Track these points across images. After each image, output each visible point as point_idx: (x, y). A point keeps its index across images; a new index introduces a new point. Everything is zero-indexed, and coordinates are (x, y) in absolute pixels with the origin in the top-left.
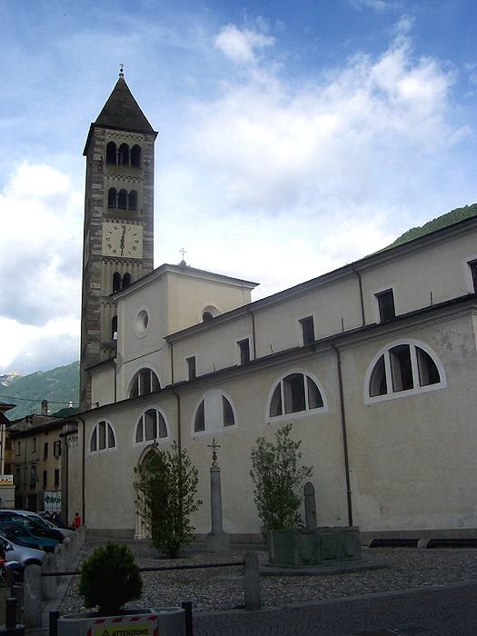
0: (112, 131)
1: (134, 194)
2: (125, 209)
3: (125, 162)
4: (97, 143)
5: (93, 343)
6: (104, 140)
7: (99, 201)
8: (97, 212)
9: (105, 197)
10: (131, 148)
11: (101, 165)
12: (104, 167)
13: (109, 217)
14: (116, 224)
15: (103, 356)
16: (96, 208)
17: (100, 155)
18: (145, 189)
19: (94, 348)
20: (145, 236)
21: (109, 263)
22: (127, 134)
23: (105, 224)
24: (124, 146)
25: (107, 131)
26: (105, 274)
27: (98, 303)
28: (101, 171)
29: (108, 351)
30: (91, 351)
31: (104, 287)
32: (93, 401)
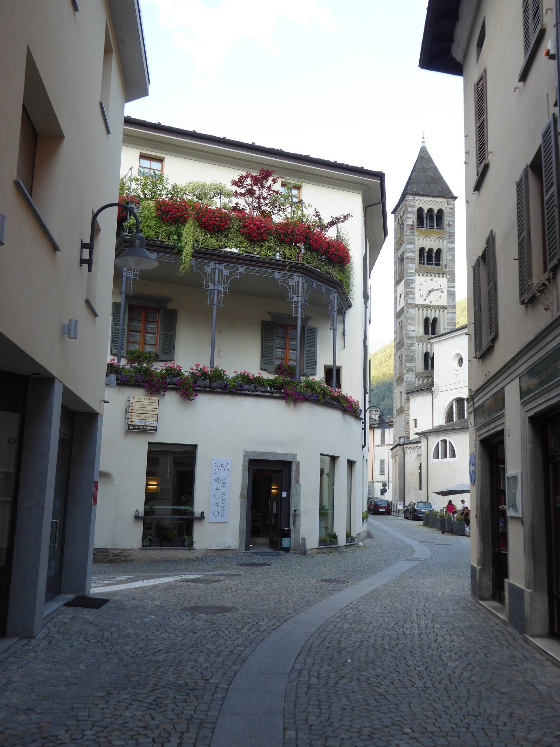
0: (421, 198)
1: (439, 251)
2: (431, 264)
3: (432, 227)
5: (410, 373)
6: (414, 206)
7: (411, 259)
8: (411, 268)
9: (416, 255)
10: (436, 212)
12: (415, 232)
13: (419, 272)
14: (425, 278)
15: (418, 383)
16: (410, 265)
17: (411, 219)
18: (448, 248)
19: (410, 377)
20: (448, 287)
21: (421, 309)
24: (430, 211)
25: (417, 198)
26: (419, 318)
27: (413, 342)
28: (413, 234)
29: (421, 379)
30: (409, 379)
31: (418, 329)
32: (412, 418)
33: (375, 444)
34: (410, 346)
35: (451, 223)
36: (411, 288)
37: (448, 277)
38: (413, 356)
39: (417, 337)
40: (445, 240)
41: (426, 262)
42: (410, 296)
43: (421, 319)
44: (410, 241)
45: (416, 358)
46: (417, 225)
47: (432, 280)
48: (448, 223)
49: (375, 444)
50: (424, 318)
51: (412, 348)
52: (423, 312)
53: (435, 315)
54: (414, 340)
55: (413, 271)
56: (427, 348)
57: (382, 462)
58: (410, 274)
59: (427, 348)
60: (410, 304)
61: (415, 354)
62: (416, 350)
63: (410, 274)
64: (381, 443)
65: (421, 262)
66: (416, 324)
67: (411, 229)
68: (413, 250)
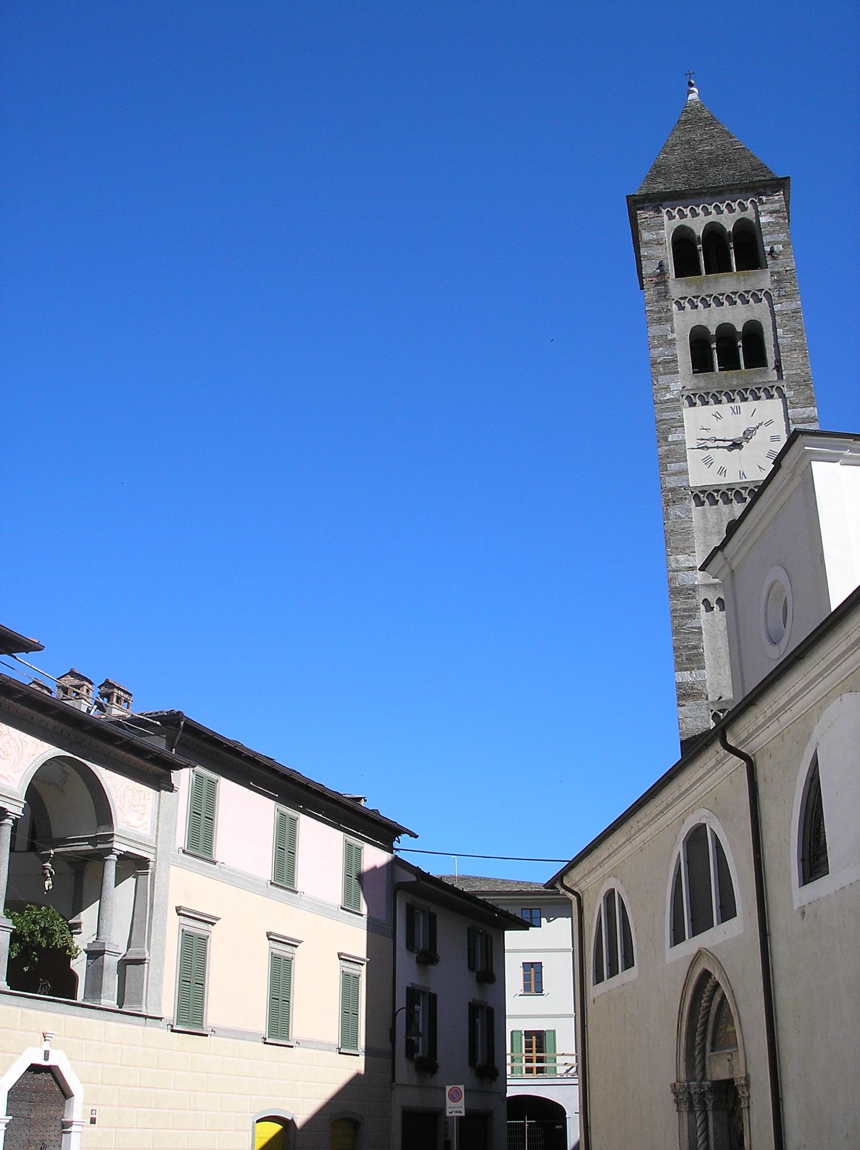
1: (753, 332)
5: (690, 703)
11: (664, 282)
14: (713, 408)
24: (713, 232)
34: (683, 617)
38: (695, 647)
41: (717, 367)
42: (673, 467)
46: (678, 275)
47: (738, 411)
60: (672, 490)
61: (701, 640)
65: (701, 363)
67: (657, 284)
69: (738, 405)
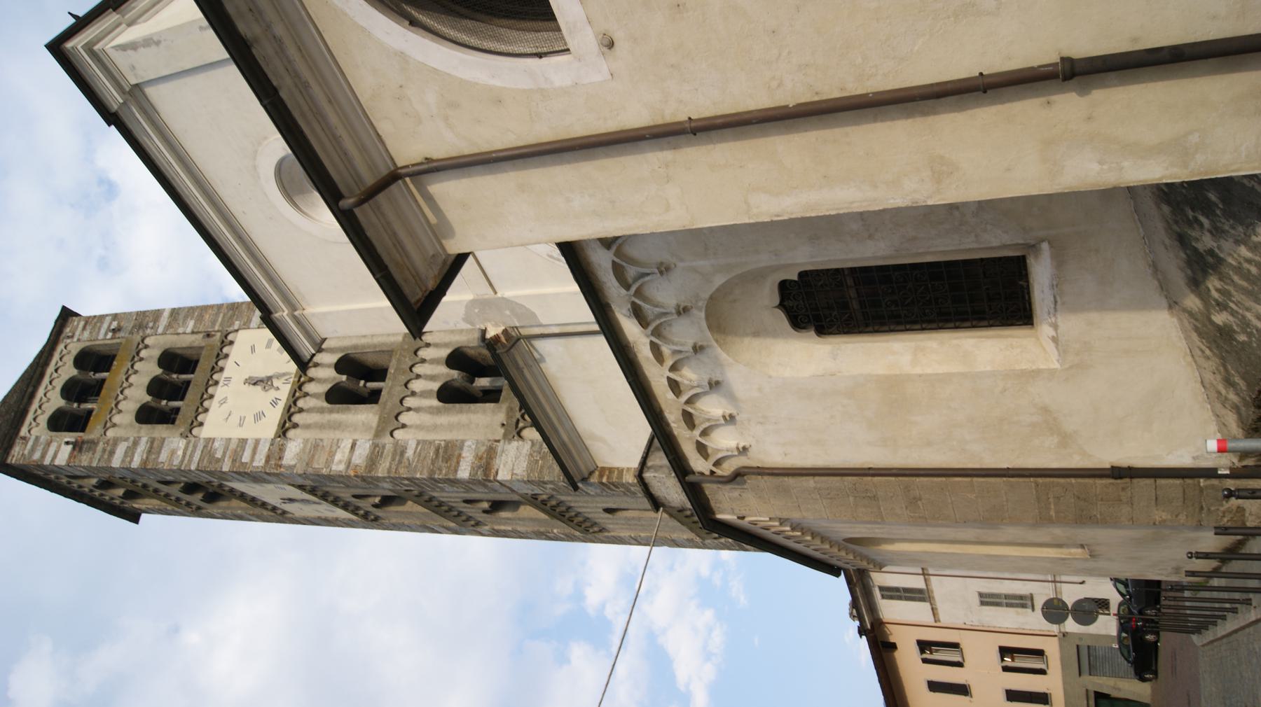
4: (37, 456)
6: (37, 438)
7: (149, 452)
8: (173, 452)
16: (163, 457)
21: (296, 418)
22: (46, 380)
23: (205, 432)
25: (24, 431)
26: (321, 427)
28: (93, 444)
33: (929, 619)
34: (400, 462)
35: (114, 325)
36: (224, 453)
37: (237, 324)
39: (378, 433)
40: (147, 341)
43: (327, 417)
44: (106, 457)
45: (449, 436)
47: (228, 379)
48: (110, 335)
49: (930, 621)
50: (325, 404)
51: (410, 453)
52: (309, 410)
53: (328, 366)
54: (384, 447)
55: (182, 443)
56: (425, 394)
57: (988, 600)
58: (187, 457)
59: (425, 394)
61: (431, 443)
62: (422, 436)
63: (187, 457)
64: (922, 600)
66: (337, 434)
67: (80, 450)
68: (130, 445)
69: (223, 379)
